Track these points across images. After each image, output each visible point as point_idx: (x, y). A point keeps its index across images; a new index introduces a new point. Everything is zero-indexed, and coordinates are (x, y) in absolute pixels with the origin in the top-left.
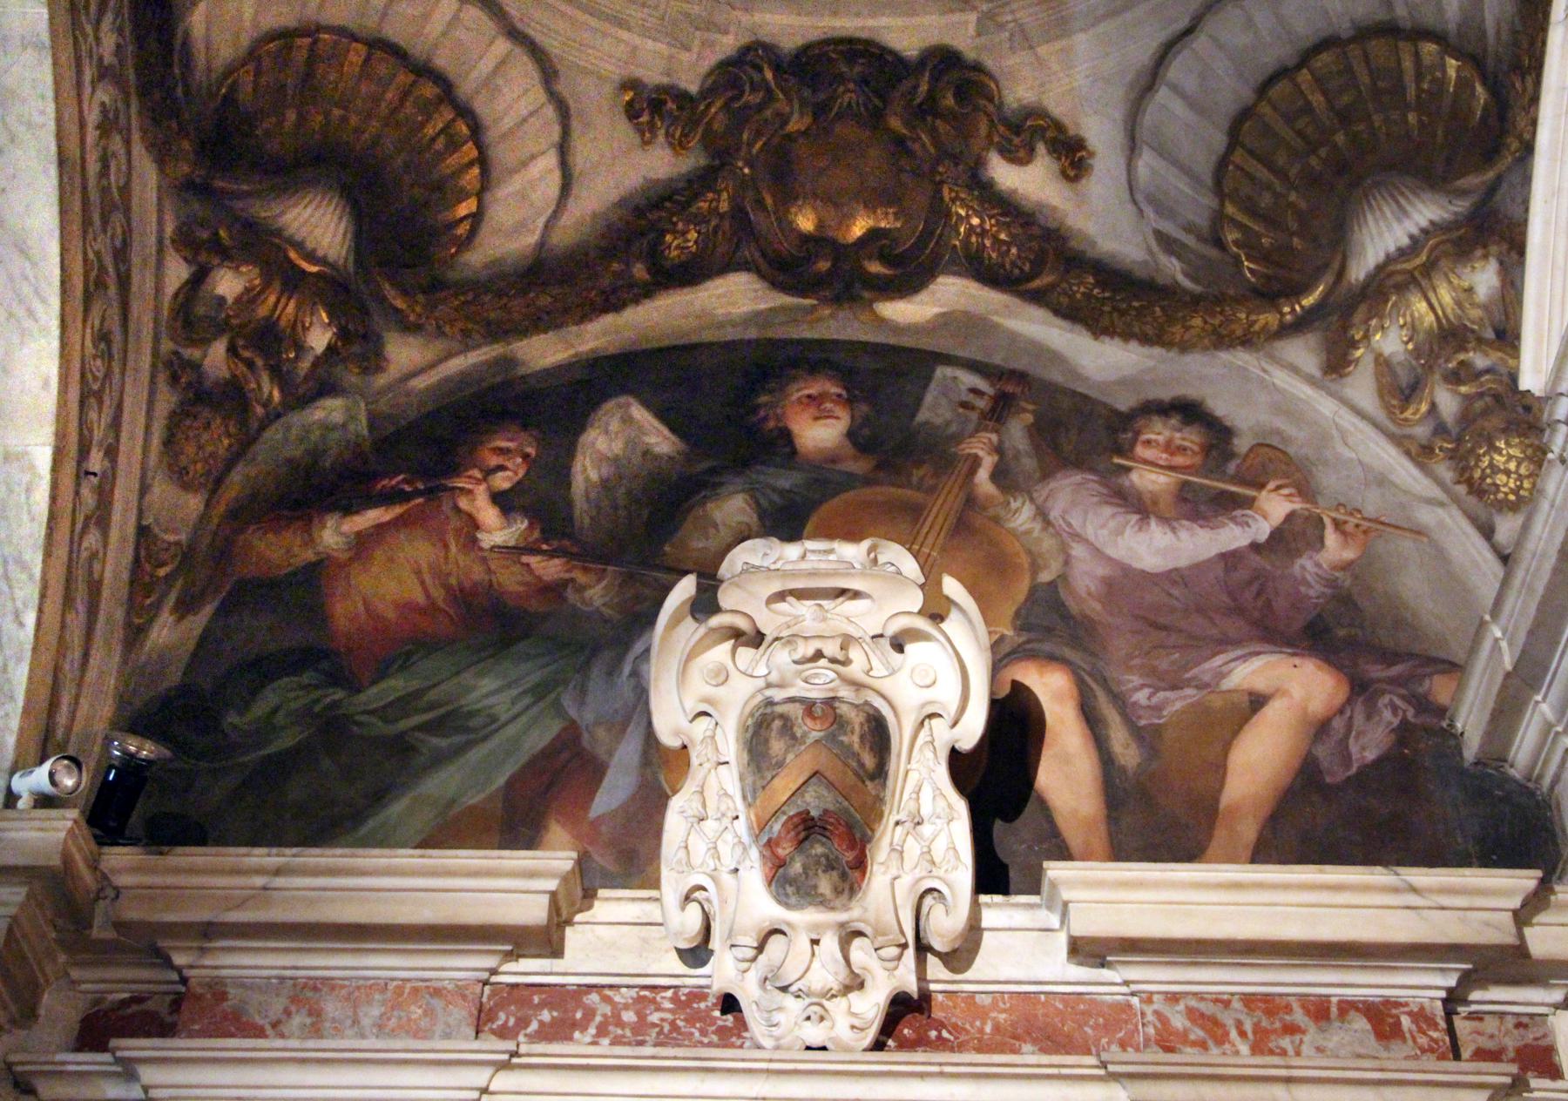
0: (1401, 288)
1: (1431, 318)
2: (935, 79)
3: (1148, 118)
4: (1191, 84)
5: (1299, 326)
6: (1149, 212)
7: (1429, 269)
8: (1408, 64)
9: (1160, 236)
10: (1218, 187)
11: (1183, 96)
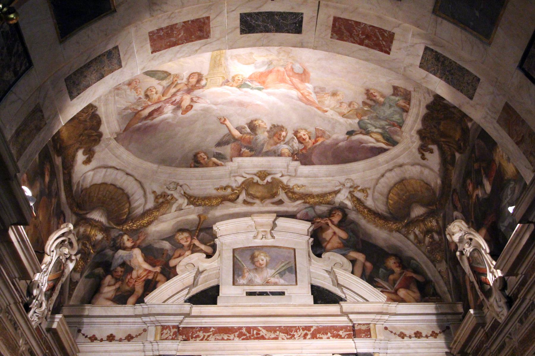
0: (90, 224)
1: (88, 232)
2: (96, 135)
3: (99, 170)
4: (108, 173)
5: (77, 214)
6: (82, 178)
7: (96, 226)
8: (123, 204)
9: (79, 181)
10: (91, 186)
11: (105, 174)
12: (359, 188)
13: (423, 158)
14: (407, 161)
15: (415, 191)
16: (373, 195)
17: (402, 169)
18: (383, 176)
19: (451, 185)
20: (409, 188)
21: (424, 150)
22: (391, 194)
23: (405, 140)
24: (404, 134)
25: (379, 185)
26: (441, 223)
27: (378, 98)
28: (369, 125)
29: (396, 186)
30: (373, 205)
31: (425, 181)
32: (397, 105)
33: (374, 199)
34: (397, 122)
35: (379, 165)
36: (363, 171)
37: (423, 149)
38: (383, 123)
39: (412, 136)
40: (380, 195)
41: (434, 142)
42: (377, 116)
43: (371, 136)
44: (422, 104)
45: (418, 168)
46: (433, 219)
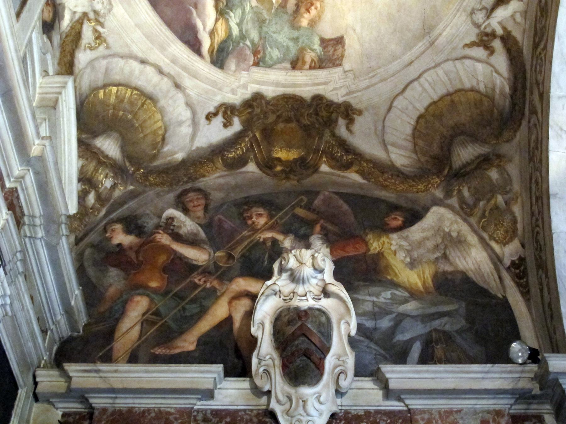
12: (99, 28)
13: (209, 117)
14: (192, 93)
15: (141, 126)
16: (97, 59)
17: (173, 90)
18: (143, 62)
19: (197, 179)
20: (143, 116)
21: (225, 113)
22: (114, 89)
23: (232, 79)
24: (244, 73)
25: (121, 62)
26: (117, 193)
27: (306, 15)
28: (239, 12)
29: (135, 92)
30: (81, 67)
31: (167, 135)
32: (302, 50)
33: (91, 63)
34: (264, 56)
35: (163, 48)
36: (137, 25)
37: (227, 111)
38: (254, 35)
39: (245, 86)
40: (103, 70)
41: (247, 125)
42: (264, 21)
43: (217, 20)
44: (321, 87)
45: (186, 114)
46: (113, 177)
